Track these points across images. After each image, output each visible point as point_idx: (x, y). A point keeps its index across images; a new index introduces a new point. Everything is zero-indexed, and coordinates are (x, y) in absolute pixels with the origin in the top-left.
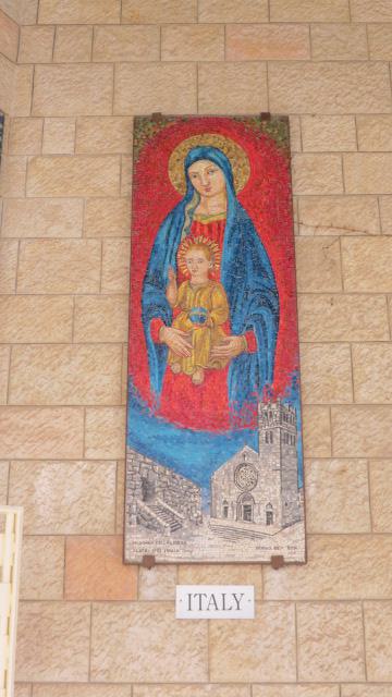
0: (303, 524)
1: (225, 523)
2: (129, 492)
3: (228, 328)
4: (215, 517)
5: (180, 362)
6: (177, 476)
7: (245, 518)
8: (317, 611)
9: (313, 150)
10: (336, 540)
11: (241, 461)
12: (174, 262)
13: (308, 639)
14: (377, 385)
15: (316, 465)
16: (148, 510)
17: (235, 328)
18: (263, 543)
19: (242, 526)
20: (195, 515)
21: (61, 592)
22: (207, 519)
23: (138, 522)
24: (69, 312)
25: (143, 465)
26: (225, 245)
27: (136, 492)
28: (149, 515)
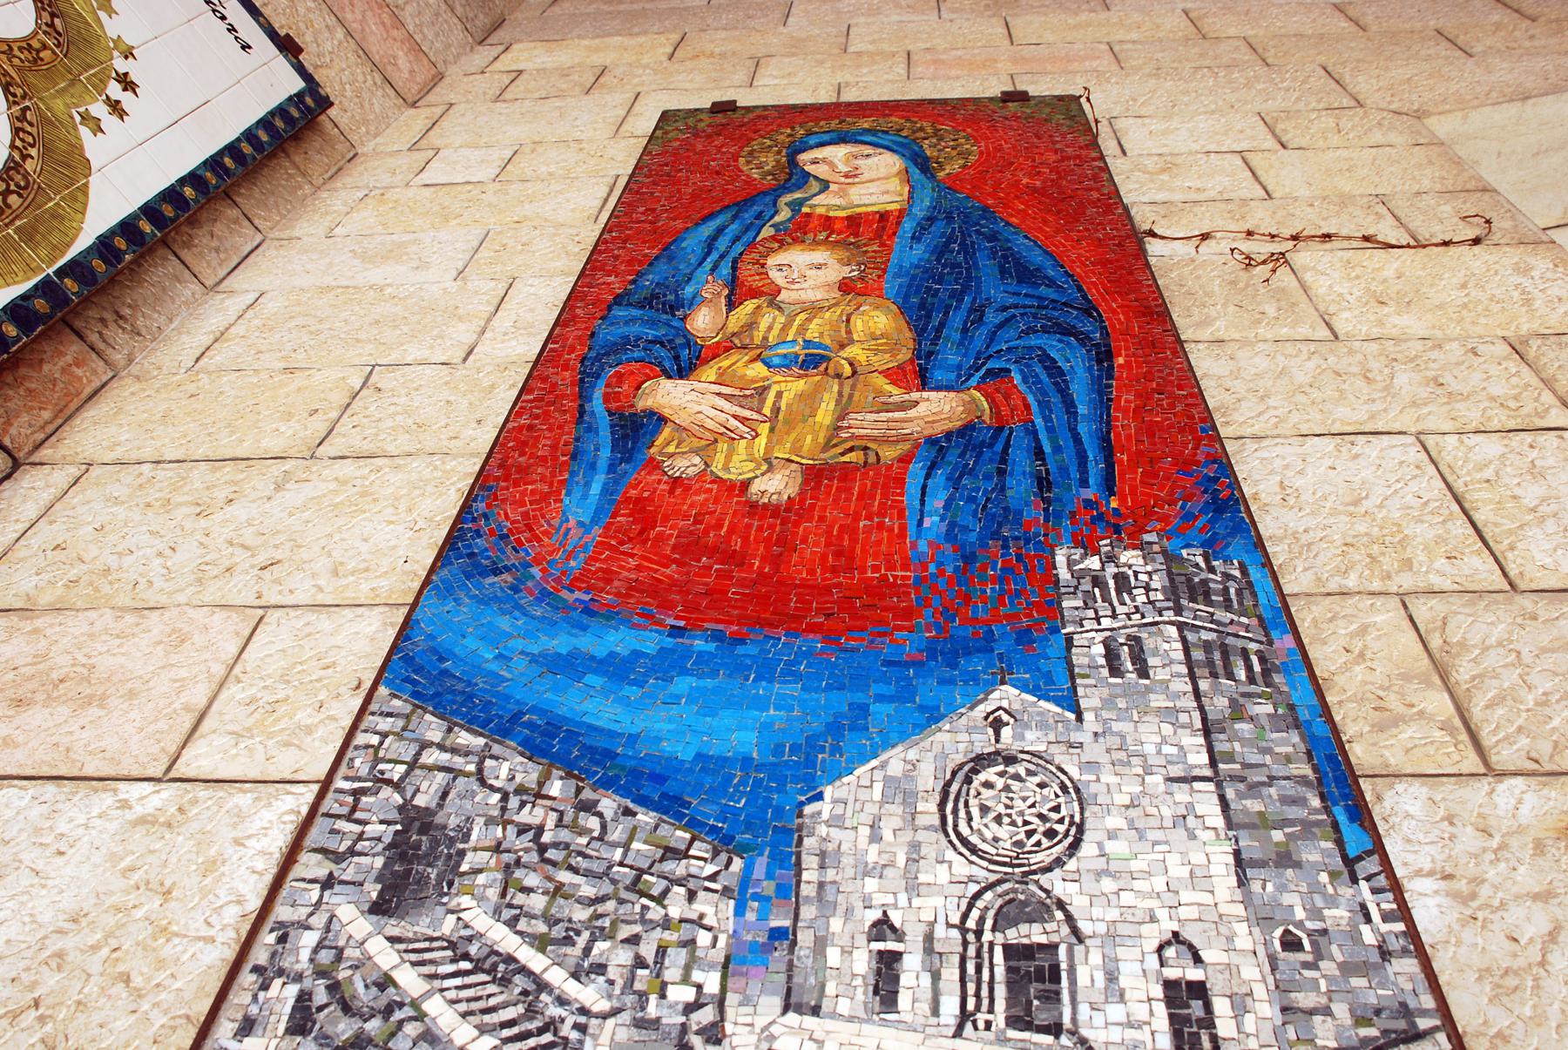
3: (919, 374)
4: (816, 1011)
9: (1154, 151)
11: (983, 742)
12: (725, 270)
16: (385, 957)
17: (939, 375)
20: (681, 994)
28: (385, 982)
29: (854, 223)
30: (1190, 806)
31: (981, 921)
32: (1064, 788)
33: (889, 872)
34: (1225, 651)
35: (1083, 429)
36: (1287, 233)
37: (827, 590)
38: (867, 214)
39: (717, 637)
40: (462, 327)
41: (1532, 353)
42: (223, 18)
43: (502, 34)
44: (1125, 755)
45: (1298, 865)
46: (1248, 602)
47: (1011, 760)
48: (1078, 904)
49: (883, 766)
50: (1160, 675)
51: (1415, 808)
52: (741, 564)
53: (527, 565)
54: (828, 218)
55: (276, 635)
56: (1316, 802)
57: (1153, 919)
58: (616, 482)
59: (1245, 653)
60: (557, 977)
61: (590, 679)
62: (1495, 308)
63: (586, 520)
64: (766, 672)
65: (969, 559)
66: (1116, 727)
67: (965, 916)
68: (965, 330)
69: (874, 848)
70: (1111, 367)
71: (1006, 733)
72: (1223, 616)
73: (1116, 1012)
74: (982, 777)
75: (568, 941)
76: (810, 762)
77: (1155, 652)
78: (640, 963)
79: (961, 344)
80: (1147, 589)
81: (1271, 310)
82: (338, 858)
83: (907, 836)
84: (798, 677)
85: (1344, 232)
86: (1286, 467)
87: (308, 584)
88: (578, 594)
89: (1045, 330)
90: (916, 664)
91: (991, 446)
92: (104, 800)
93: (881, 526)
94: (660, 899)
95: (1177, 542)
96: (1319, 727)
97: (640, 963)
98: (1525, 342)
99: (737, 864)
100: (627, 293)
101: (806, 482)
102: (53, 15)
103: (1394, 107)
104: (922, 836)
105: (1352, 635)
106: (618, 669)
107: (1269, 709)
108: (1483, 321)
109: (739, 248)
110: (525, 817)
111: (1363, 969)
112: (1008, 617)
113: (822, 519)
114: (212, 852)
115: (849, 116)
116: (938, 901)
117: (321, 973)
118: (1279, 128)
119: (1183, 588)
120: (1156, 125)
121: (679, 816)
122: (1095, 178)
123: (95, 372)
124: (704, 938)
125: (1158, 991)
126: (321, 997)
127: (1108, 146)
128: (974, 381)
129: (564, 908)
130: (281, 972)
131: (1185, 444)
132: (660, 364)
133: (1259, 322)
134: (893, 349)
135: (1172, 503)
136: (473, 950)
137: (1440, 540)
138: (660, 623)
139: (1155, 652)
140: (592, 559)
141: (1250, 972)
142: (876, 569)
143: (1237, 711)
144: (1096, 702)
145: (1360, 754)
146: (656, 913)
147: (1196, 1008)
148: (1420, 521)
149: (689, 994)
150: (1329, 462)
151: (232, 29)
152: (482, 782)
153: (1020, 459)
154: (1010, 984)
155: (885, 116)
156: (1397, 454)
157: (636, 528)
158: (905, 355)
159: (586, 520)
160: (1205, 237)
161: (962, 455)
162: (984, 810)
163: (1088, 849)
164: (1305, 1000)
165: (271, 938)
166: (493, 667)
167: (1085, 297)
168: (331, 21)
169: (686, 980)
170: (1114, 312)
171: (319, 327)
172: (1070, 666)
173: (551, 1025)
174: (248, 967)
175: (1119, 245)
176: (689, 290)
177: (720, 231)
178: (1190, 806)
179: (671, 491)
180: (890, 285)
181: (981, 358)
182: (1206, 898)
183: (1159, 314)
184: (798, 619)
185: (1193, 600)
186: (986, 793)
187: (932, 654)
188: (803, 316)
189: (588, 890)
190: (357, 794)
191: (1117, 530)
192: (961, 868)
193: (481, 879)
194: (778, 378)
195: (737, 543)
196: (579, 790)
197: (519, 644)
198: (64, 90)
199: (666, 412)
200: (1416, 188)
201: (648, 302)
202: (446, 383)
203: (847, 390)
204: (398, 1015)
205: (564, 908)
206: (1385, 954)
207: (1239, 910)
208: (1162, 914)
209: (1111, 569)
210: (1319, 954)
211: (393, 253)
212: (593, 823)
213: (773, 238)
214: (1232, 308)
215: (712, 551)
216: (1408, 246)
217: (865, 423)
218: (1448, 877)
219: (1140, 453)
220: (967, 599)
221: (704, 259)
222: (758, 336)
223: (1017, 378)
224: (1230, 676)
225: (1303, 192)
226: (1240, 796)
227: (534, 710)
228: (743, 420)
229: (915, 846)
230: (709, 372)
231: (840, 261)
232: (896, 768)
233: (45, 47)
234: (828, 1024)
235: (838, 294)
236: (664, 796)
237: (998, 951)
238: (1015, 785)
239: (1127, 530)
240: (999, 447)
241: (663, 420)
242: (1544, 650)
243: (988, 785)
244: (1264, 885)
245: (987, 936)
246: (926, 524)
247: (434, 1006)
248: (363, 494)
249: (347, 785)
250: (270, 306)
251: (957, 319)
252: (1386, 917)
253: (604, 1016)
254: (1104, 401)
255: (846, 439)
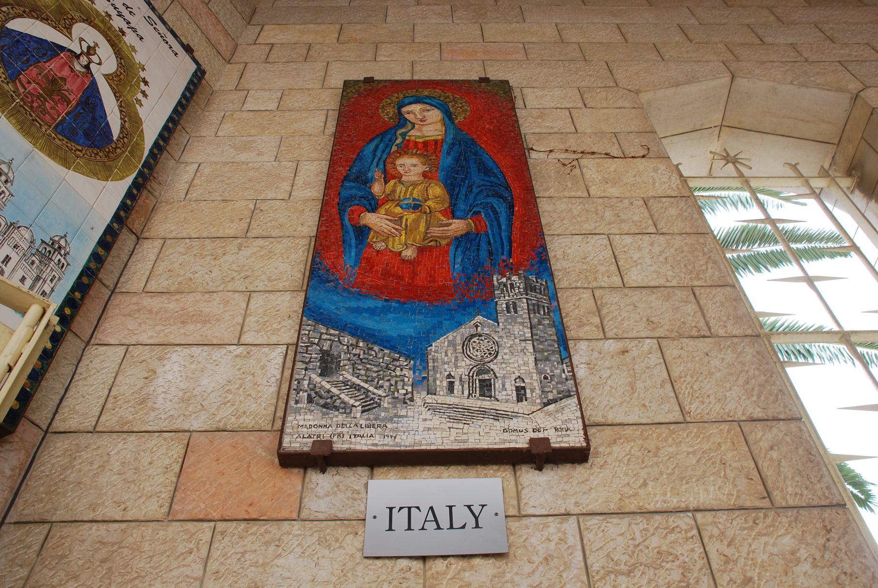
0: (575, 400)
1: (450, 400)
2: (299, 365)
3: (452, 213)
4: (435, 394)
5: (386, 240)
6: (376, 348)
7: (482, 395)
8: (616, 527)
9: (537, 107)
10: (629, 431)
11: (473, 331)
12: (382, 166)
13: (609, 573)
14: (652, 269)
15: (583, 345)
16: (328, 386)
17: (458, 213)
18: (513, 424)
19: (479, 403)
21: (165, 509)
22: (420, 397)
23: (310, 400)
24: (247, 213)
25: (325, 337)
26: (443, 155)
27: (311, 366)
28: (329, 391)
29: (426, 144)
30: (525, 347)
31: (473, 374)
32: (494, 343)
33: (450, 363)
34: (538, 306)
35: (503, 234)
36: (580, 150)
37: (428, 288)
38: (430, 140)
39: (398, 302)
40: (285, 184)
41: (650, 204)
42: (167, 43)
43: (256, 19)
44: (509, 334)
45: (550, 361)
46: (546, 292)
47: (480, 336)
48: (496, 370)
49: (447, 337)
50: (521, 313)
51: (584, 348)
52: (402, 280)
53: (337, 280)
54: (416, 142)
55: (257, 302)
56: (556, 346)
57: (514, 373)
58: (359, 252)
59: (544, 307)
60: (371, 389)
61: (364, 314)
62: (643, 186)
63: (352, 265)
64: (413, 312)
65: (469, 278)
66: (508, 327)
67: (469, 373)
68: (466, 195)
69: (446, 358)
70: (513, 211)
71: (479, 328)
72: (539, 296)
73: (504, 393)
74: (473, 340)
75: (372, 381)
76: (428, 337)
77: (520, 307)
78: (391, 385)
79: (465, 201)
80: (519, 288)
81: (569, 184)
82: (307, 363)
83: (454, 355)
84: (422, 314)
85: (600, 151)
86: (566, 246)
87: (262, 284)
88: (355, 289)
89: (493, 196)
90: (455, 310)
91: (475, 240)
92: (223, 351)
93: (442, 267)
94: (394, 371)
95: (528, 273)
96: (560, 327)
97: (391, 385)
98: (648, 200)
99: (412, 362)
100: (348, 175)
101: (418, 252)
102: (121, 59)
103: (629, 87)
104: (458, 355)
105: (576, 301)
106: (372, 311)
107: (548, 322)
108: (638, 191)
109: (385, 156)
110: (354, 351)
111: (561, 383)
112: (480, 296)
113: (425, 265)
114: (262, 364)
115: (420, 88)
116: (463, 370)
117: (311, 390)
118: (585, 96)
119: (529, 288)
120: (539, 93)
121: (396, 351)
122: (513, 126)
123: (151, 201)
124: (406, 379)
125: (514, 388)
126: (313, 395)
127: (519, 103)
128: (469, 216)
129: (369, 373)
130: (301, 390)
131: (534, 240)
132: (365, 207)
133: (564, 189)
134: (443, 202)
135: (528, 261)
136: (349, 383)
137: (607, 271)
138: (381, 298)
139: (520, 307)
140: (357, 278)
141: (536, 384)
142: (442, 281)
143: (540, 323)
144: (503, 320)
145: (570, 334)
146: (393, 374)
147: (523, 392)
148: (602, 265)
149: (404, 392)
150: (579, 244)
151: (171, 47)
152: (341, 343)
153: (484, 245)
154: (480, 388)
155: (434, 88)
156: (600, 242)
157: (368, 268)
158: (447, 205)
159: (352, 265)
160: (551, 151)
161: (466, 243)
162: (474, 348)
163: (499, 357)
164: (547, 389)
165: (296, 383)
166: (335, 311)
167: (506, 182)
168: (195, 27)
169: (403, 388)
170: (516, 191)
171: (228, 181)
172: (497, 311)
173: (372, 399)
174: (292, 389)
175: (520, 159)
176: (370, 175)
177: (377, 147)
178: (525, 347)
179: (377, 255)
180: (440, 175)
181: (472, 206)
182: (527, 368)
183: (530, 190)
184: (421, 297)
185: (531, 291)
186: (474, 344)
187: (459, 307)
188: (411, 188)
189: (375, 369)
190: (307, 347)
191: (511, 269)
192: (468, 362)
193: (347, 367)
194: (405, 213)
195: (400, 273)
196: (367, 345)
197: (341, 305)
198: (129, 90)
199: (371, 226)
200: (629, 130)
201: (356, 180)
202: (286, 208)
203: (428, 219)
204: (334, 398)
205: (369, 373)
206: (567, 379)
207: (535, 371)
208: (516, 372)
209: (509, 282)
210: (552, 380)
211: (245, 147)
212: (373, 353)
213: (397, 151)
214: (556, 183)
215: (393, 276)
216: (621, 158)
217: (436, 231)
218: (589, 364)
219: (520, 243)
220: (468, 291)
221: (373, 161)
222: (397, 195)
223: (483, 214)
224: (539, 313)
225: (589, 131)
226: (538, 344)
227: (350, 323)
228: (396, 229)
229: (456, 357)
230: (382, 210)
231: (422, 163)
232: (451, 338)
233: (121, 73)
234: (438, 397)
235: (422, 178)
236: (391, 346)
237: (477, 381)
238: (481, 342)
239: (513, 269)
240: (477, 241)
241: (370, 229)
242: (627, 305)
243: (474, 342)
244: (541, 366)
245: (475, 377)
246: (456, 267)
247: (342, 396)
248: (270, 252)
249: (303, 345)
250: (206, 170)
251: (463, 191)
252: (569, 372)
253: (385, 397)
254: (510, 224)
255: (430, 237)
